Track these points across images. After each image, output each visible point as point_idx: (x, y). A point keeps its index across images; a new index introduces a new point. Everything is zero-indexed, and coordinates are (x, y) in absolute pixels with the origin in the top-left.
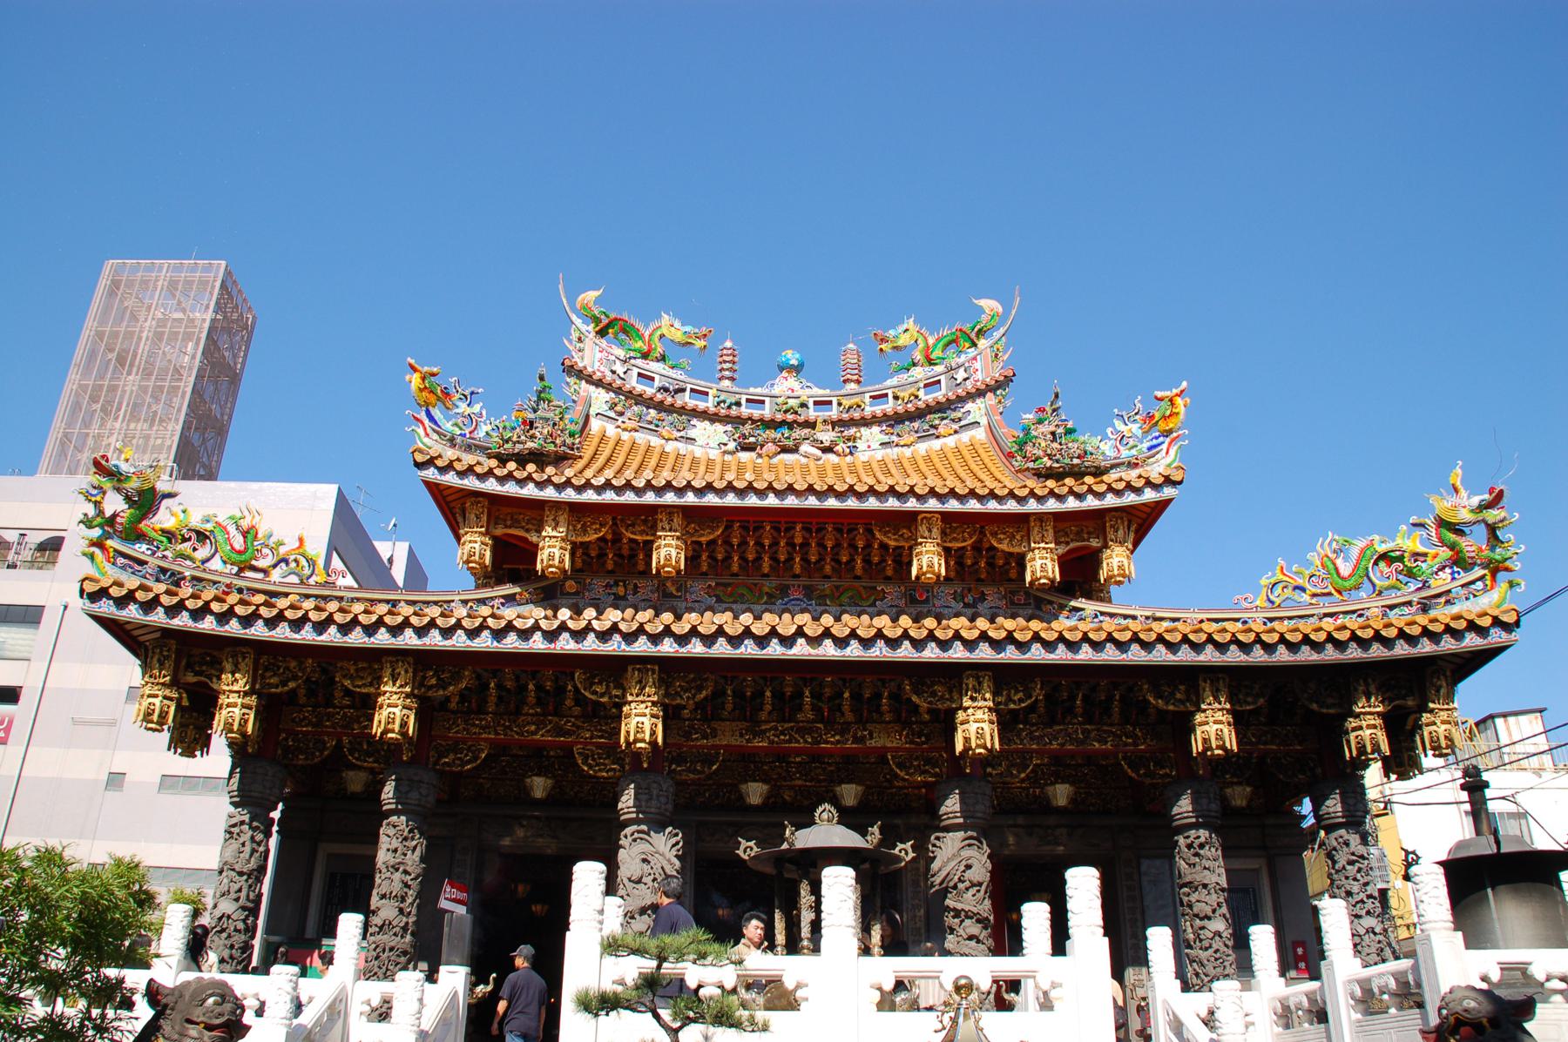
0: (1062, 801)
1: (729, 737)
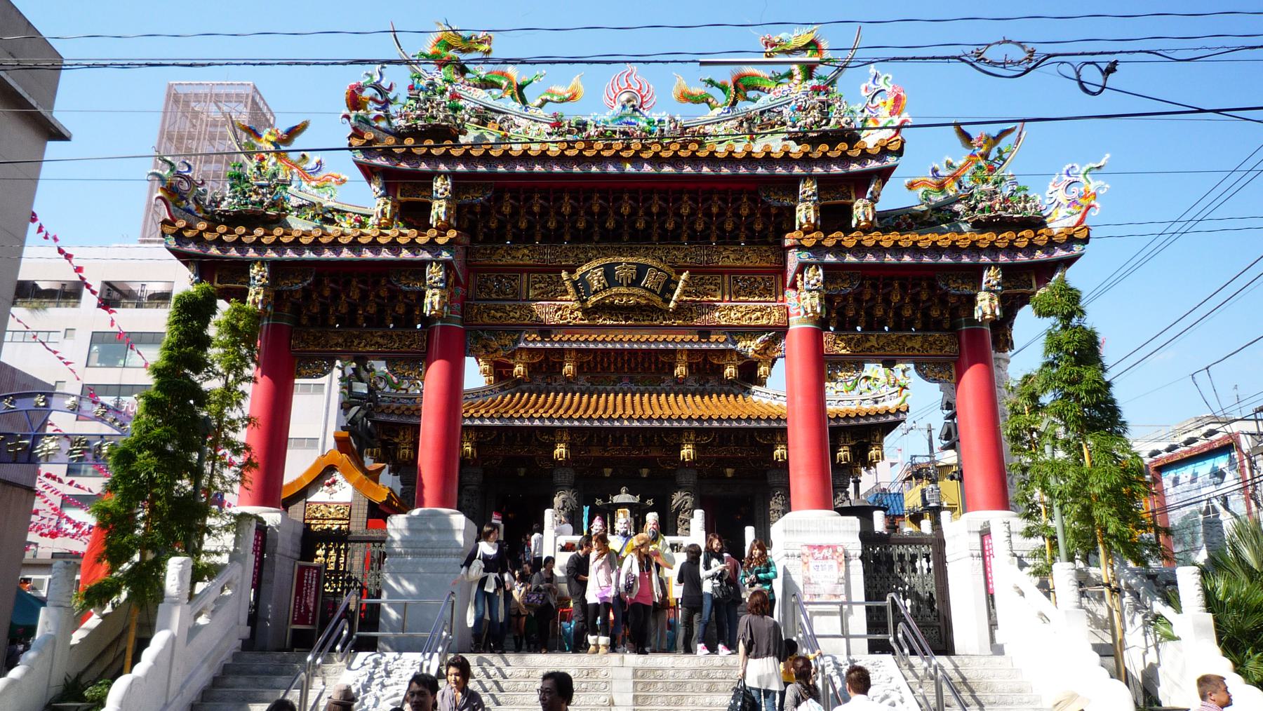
0: (729, 475)
1: (596, 452)
